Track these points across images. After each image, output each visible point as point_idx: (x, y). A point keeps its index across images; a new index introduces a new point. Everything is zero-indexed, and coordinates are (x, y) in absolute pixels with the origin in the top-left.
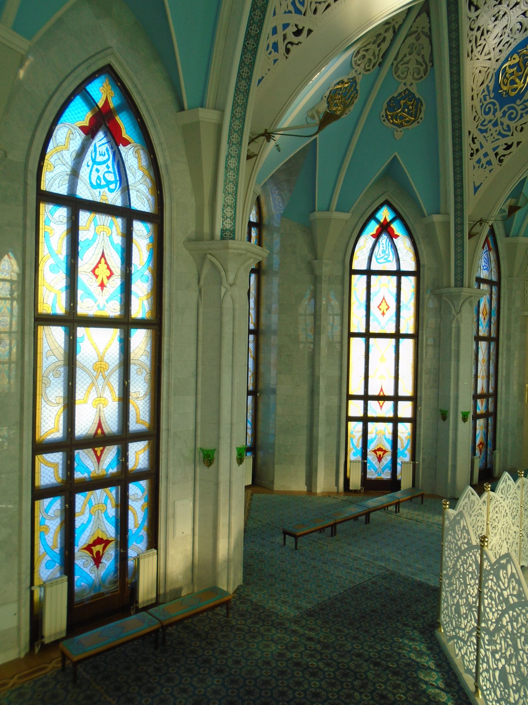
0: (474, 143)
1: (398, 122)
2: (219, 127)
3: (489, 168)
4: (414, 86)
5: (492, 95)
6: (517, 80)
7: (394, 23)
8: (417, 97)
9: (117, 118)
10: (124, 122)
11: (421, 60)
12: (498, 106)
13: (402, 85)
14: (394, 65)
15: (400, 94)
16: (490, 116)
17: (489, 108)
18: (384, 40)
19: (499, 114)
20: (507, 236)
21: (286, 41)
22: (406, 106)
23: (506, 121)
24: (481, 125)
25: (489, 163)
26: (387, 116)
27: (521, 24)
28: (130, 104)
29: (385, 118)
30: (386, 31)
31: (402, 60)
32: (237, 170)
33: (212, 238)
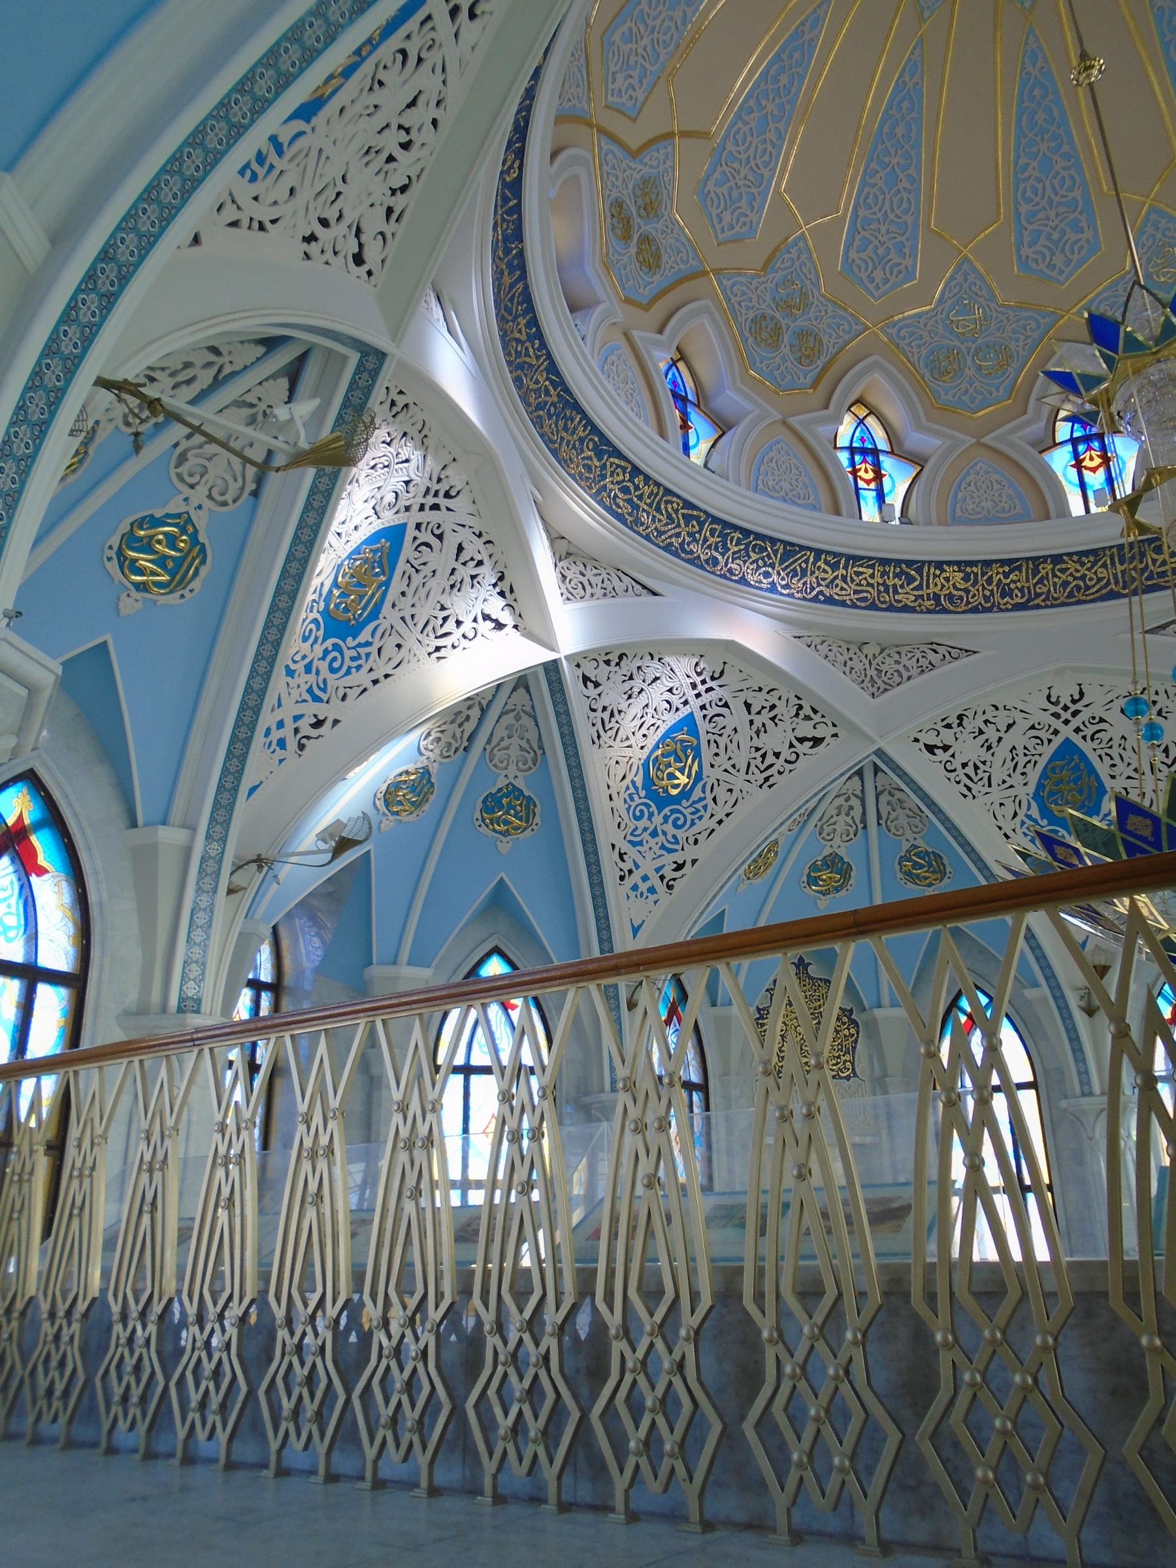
0: (623, 861)
1: (503, 828)
2: (188, 851)
3: (652, 898)
4: (520, 779)
5: (643, 793)
6: (678, 774)
7: (479, 699)
8: (526, 794)
9: (34, 839)
10: (43, 845)
11: (526, 746)
12: (654, 808)
13: (502, 777)
14: (488, 751)
15: (500, 790)
16: (644, 822)
17: (641, 811)
18: (468, 718)
19: (658, 819)
20: (714, 1004)
21: (299, 736)
22: (511, 806)
23: (669, 828)
24: (631, 834)
25: (652, 890)
26: (483, 820)
27: (668, 702)
28: (54, 818)
29: (480, 822)
30: (469, 708)
31: (498, 744)
32: (211, 909)
33: (164, 1009)
